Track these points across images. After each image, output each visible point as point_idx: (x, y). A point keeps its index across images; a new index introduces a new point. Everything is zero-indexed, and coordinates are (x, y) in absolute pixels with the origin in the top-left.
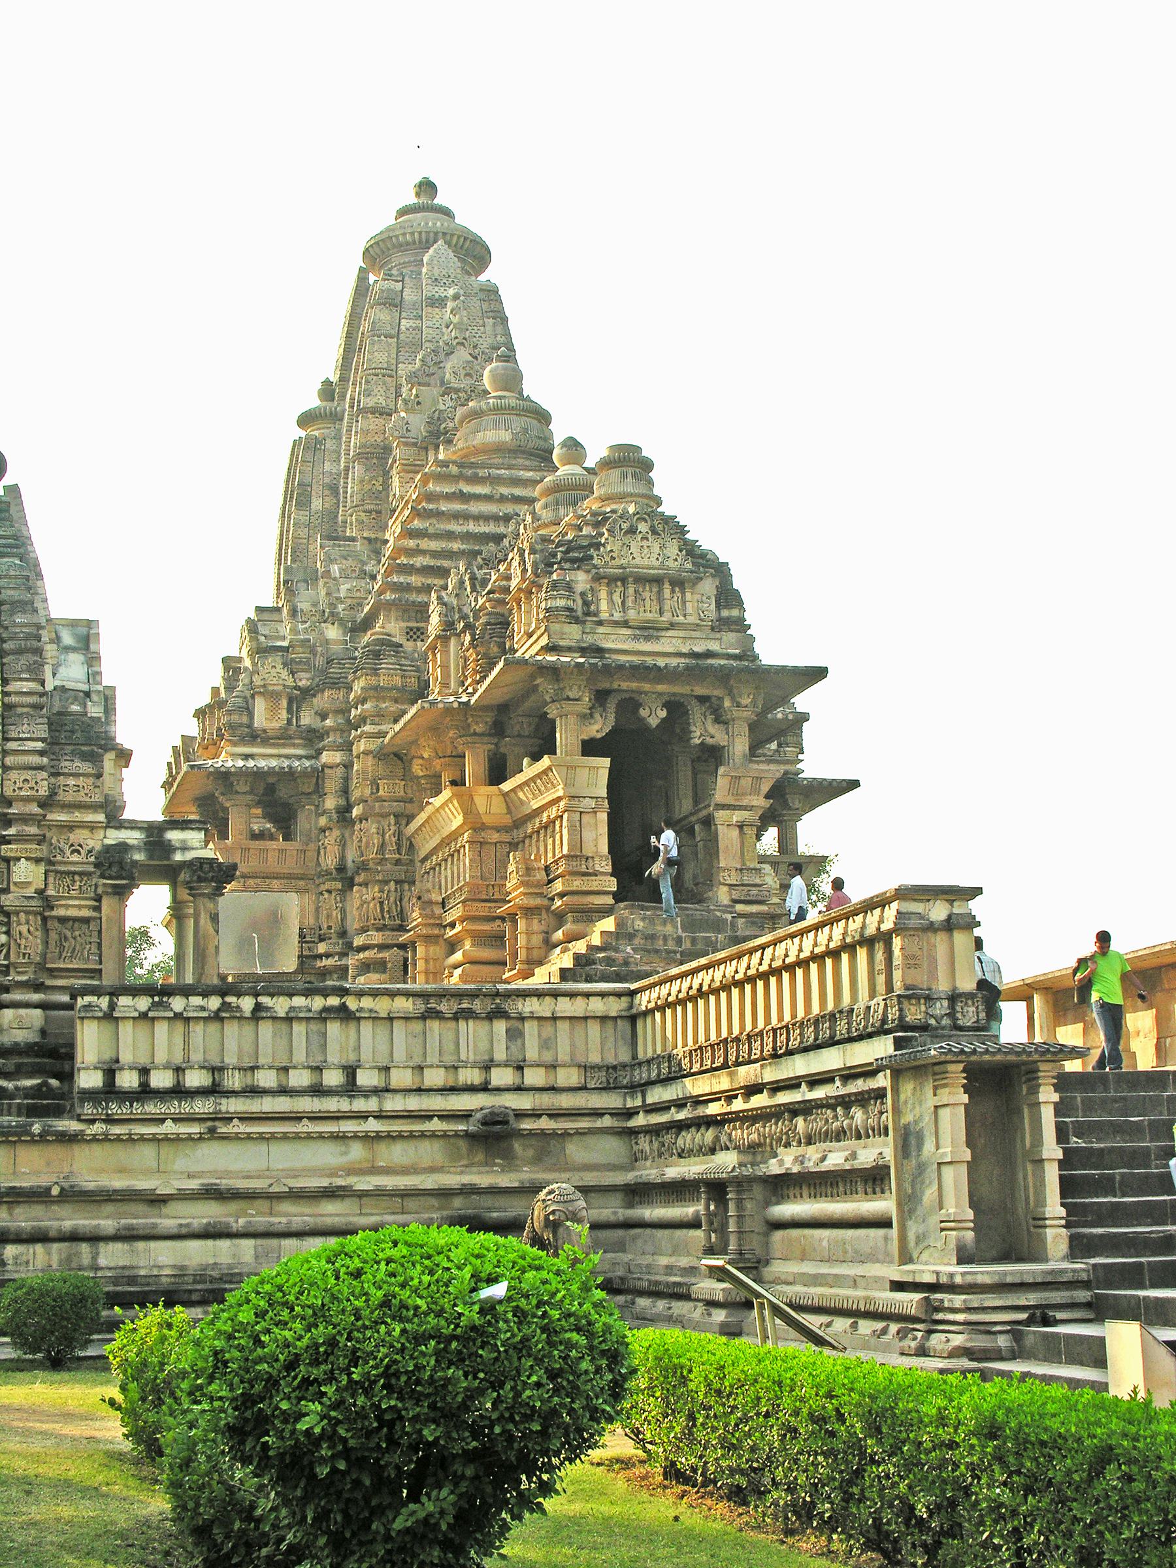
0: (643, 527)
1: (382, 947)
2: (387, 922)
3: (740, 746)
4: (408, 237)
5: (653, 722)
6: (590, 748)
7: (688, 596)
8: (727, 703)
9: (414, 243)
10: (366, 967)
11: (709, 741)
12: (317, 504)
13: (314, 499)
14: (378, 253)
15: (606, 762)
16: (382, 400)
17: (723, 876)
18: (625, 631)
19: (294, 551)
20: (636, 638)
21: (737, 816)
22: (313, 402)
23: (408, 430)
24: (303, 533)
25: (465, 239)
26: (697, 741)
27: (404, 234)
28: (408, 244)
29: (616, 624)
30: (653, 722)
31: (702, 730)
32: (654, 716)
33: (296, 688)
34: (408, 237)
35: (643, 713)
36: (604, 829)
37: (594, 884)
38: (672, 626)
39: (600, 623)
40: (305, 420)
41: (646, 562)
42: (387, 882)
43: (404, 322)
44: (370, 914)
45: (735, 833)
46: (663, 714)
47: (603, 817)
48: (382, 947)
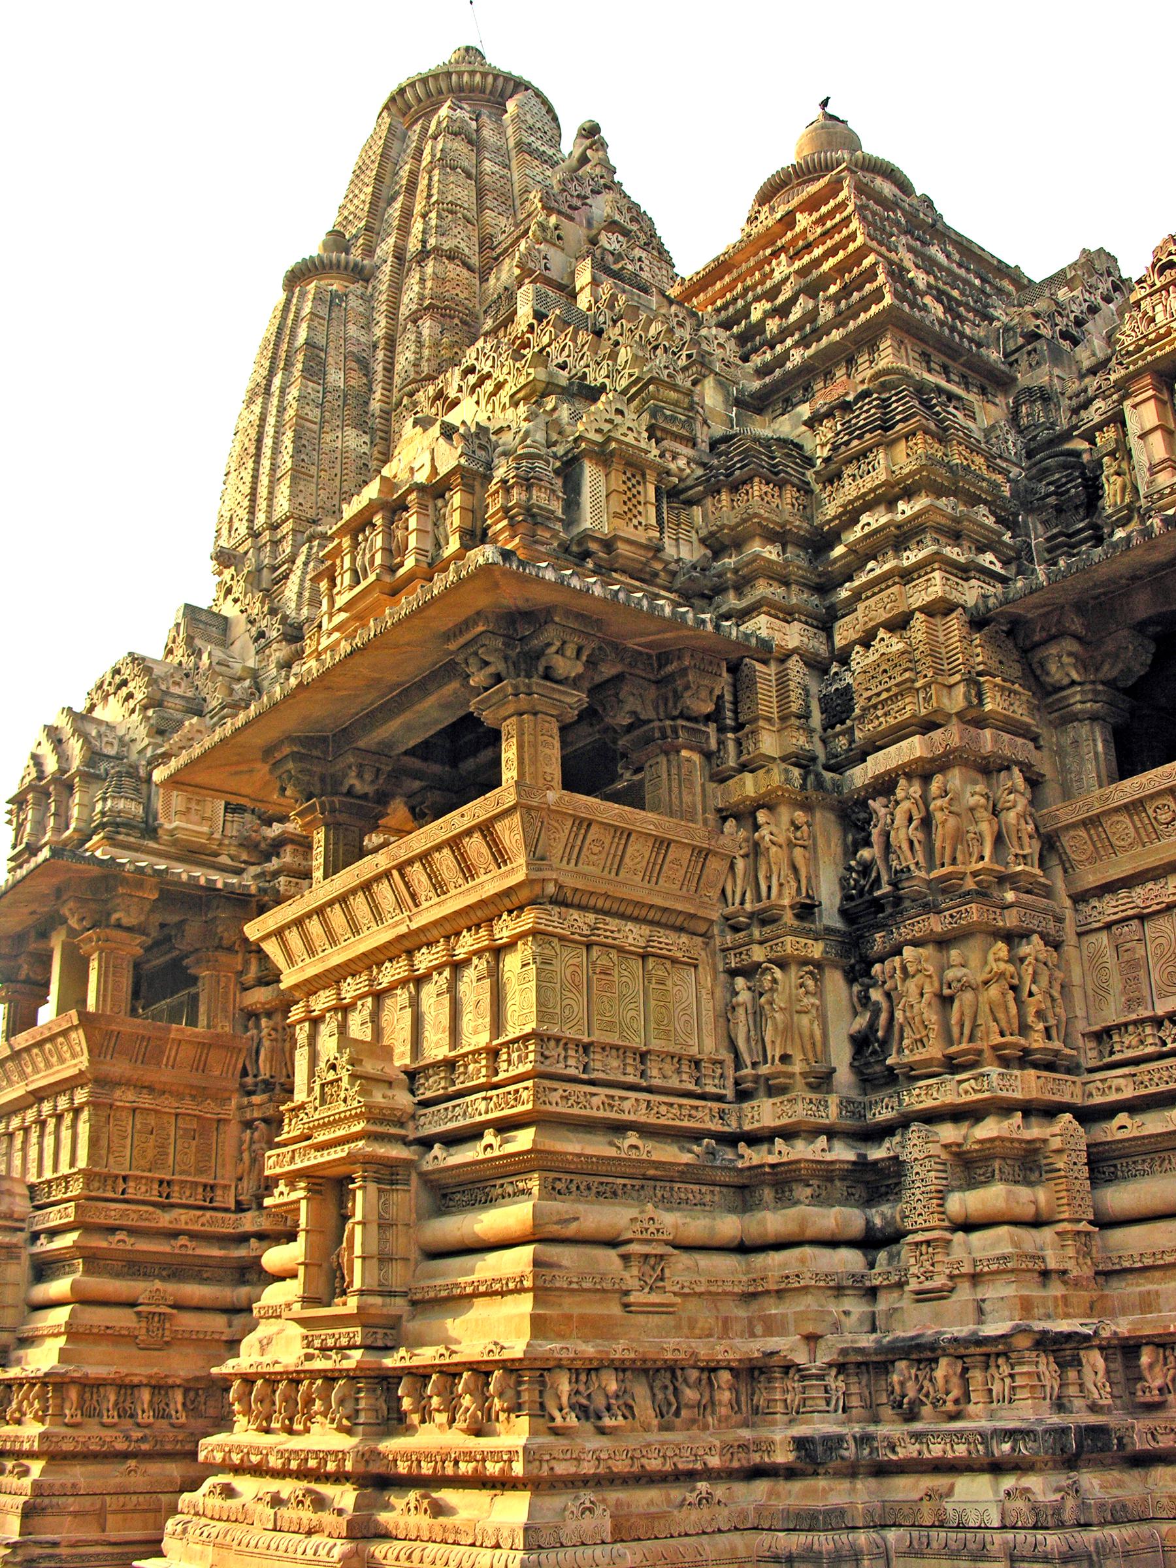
1: (1031, 1110)
2: (1037, 1041)
4: (478, 78)
9: (483, 91)
10: (969, 1167)
12: (336, 378)
13: (331, 370)
14: (409, 105)
16: (463, 245)
19: (297, 438)
23: (547, 268)
24: (314, 413)
27: (472, 73)
28: (472, 89)
34: (478, 78)
42: (1025, 935)
43: (487, 163)
44: (984, 1018)
48: (1031, 1110)
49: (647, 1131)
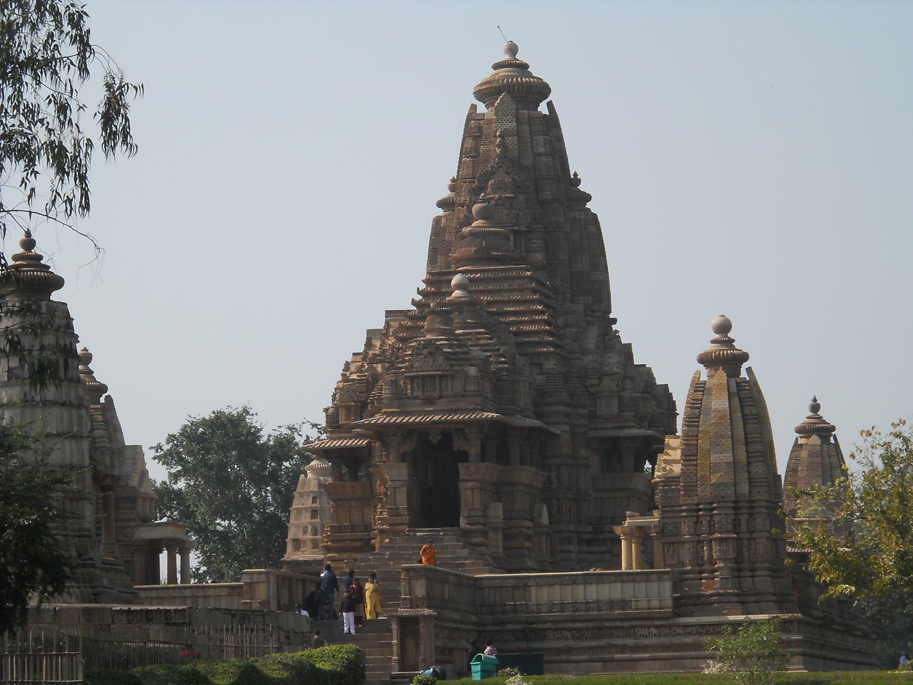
0: (425, 351)
3: (474, 451)
5: (435, 442)
6: (403, 458)
7: (449, 381)
8: (467, 431)
11: (461, 449)
15: (405, 465)
17: (462, 512)
18: (418, 401)
20: (424, 404)
21: (470, 484)
22: (446, 193)
25: (523, 86)
26: (455, 449)
29: (415, 398)
30: (435, 442)
31: (458, 444)
32: (435, 438)
33: (360, 402)
35: (430, 438)
36: (405, 495)
37: (399, 520)
38: (441, 397)
39: (408, 398)
40: (442, 204)
41: (426, 369)
45: (469, 493)
46: (439, 438)
47: (405, 489)
49: (350, 540)
